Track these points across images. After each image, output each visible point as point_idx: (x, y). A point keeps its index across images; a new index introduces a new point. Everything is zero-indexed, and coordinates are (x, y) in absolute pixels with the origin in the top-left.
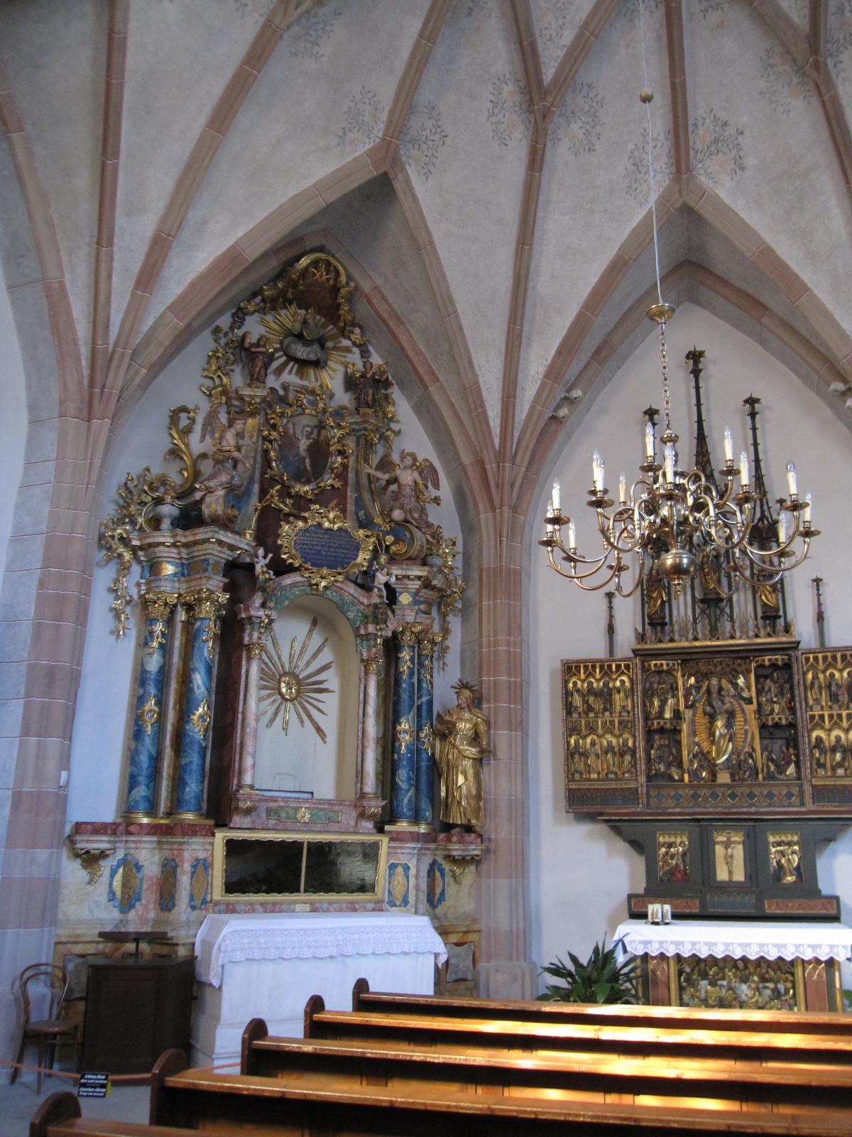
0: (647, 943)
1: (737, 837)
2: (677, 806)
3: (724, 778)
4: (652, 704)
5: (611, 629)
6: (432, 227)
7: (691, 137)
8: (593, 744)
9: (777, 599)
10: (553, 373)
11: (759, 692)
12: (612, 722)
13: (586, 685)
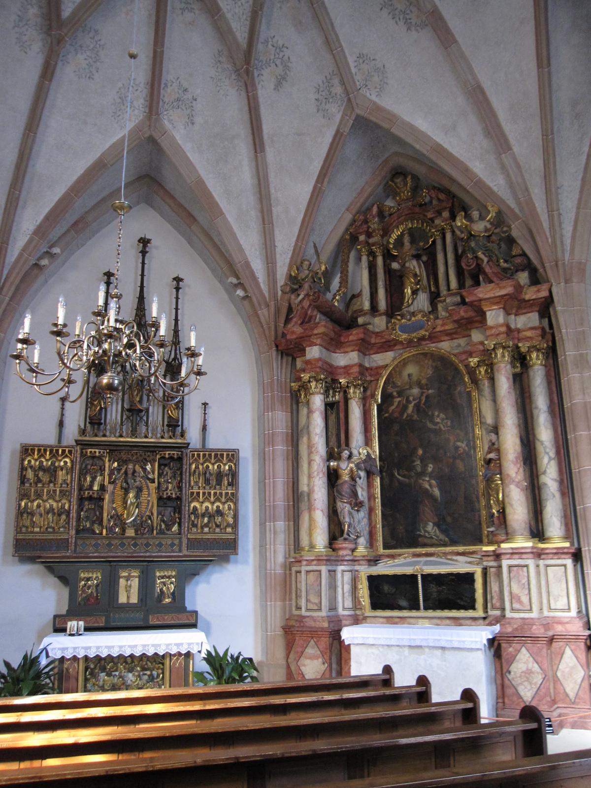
0: (63, 649)
1: (135, 573)
2: (96, 551)
3: (130, 532)
4: (85, 479)
5: (61, 424)
7: (162, 91)
8: (39, 506)
9: (178, 414)
10: (40, 232)
11: (160, 475)
12: (55, 491)
13: (38, 463)
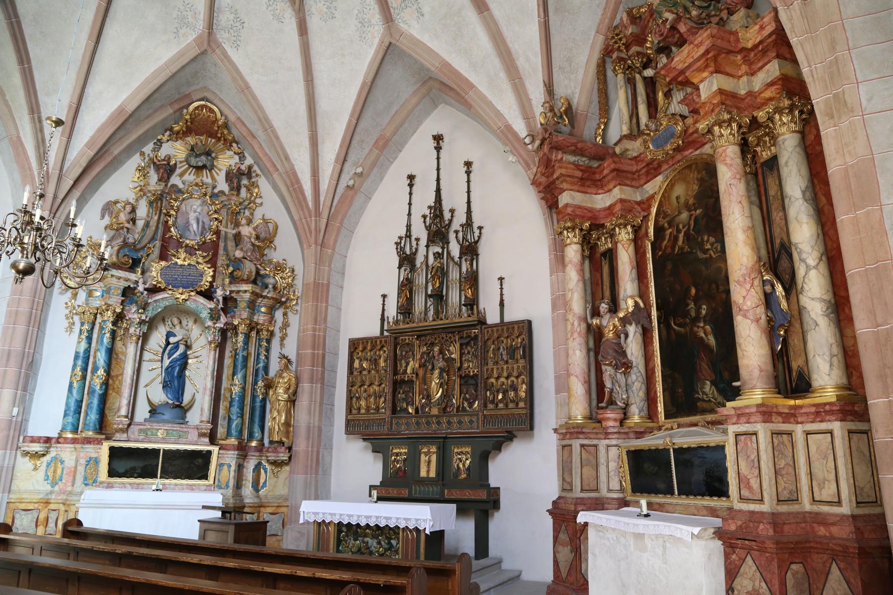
1: (434, 449)
3: (435, 411)
6: (248, 79)
8: (365, 391)
10: (343, 160)
